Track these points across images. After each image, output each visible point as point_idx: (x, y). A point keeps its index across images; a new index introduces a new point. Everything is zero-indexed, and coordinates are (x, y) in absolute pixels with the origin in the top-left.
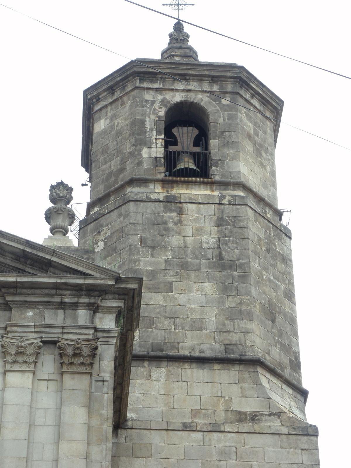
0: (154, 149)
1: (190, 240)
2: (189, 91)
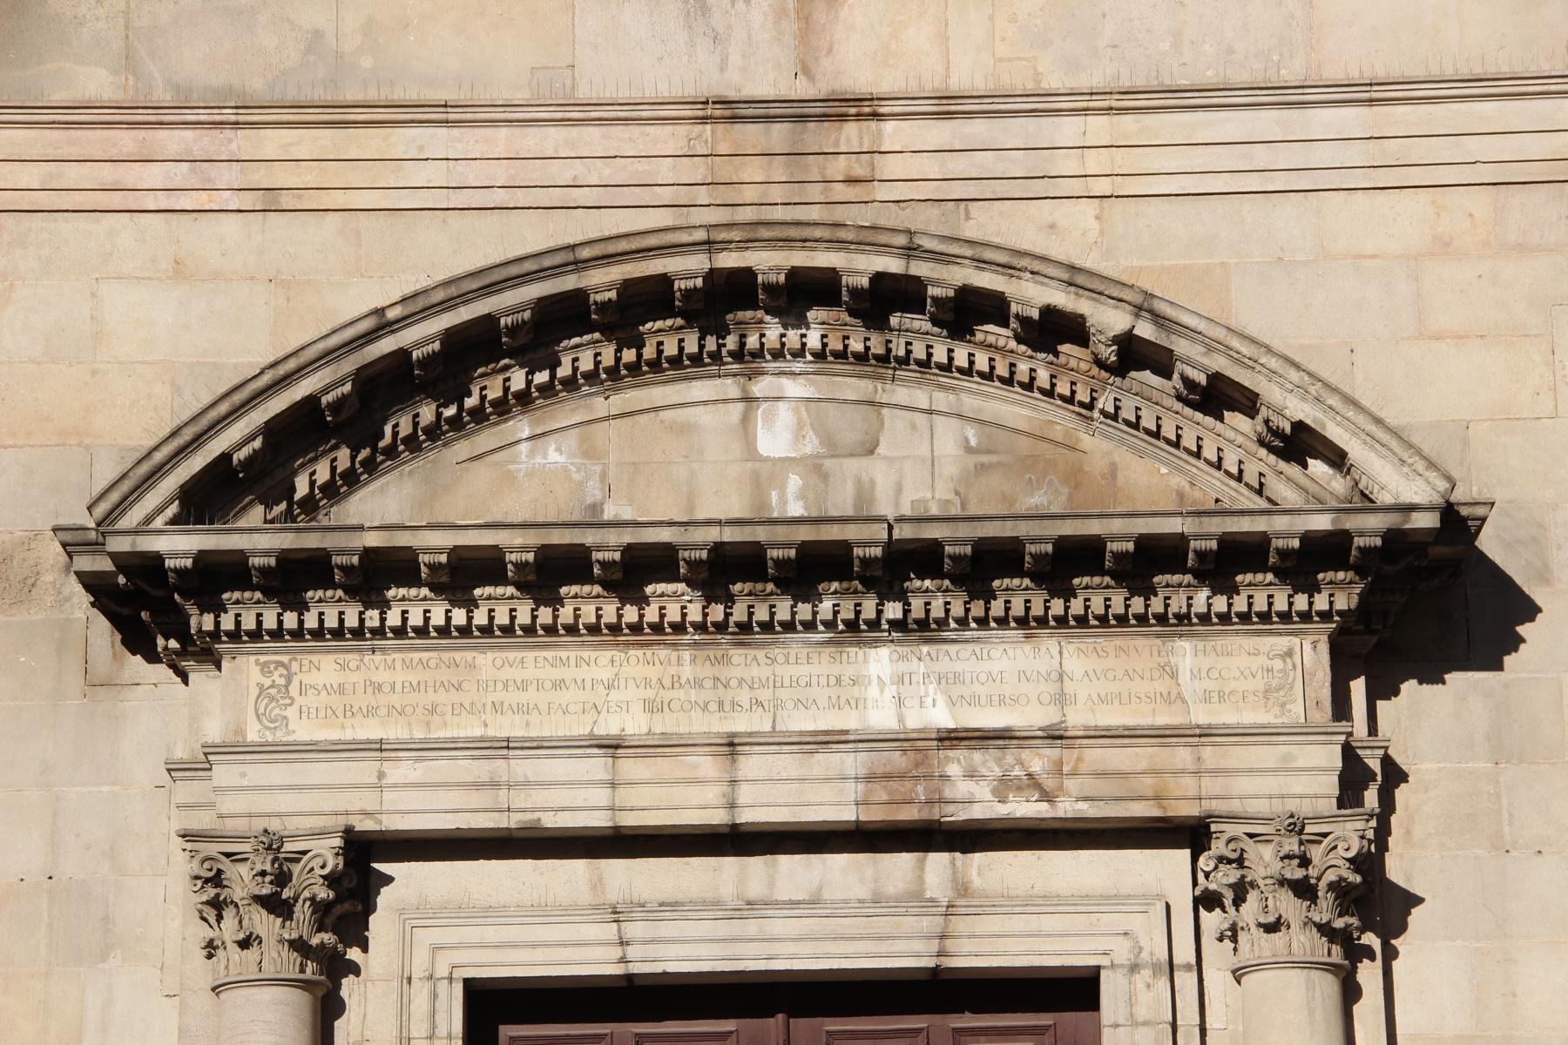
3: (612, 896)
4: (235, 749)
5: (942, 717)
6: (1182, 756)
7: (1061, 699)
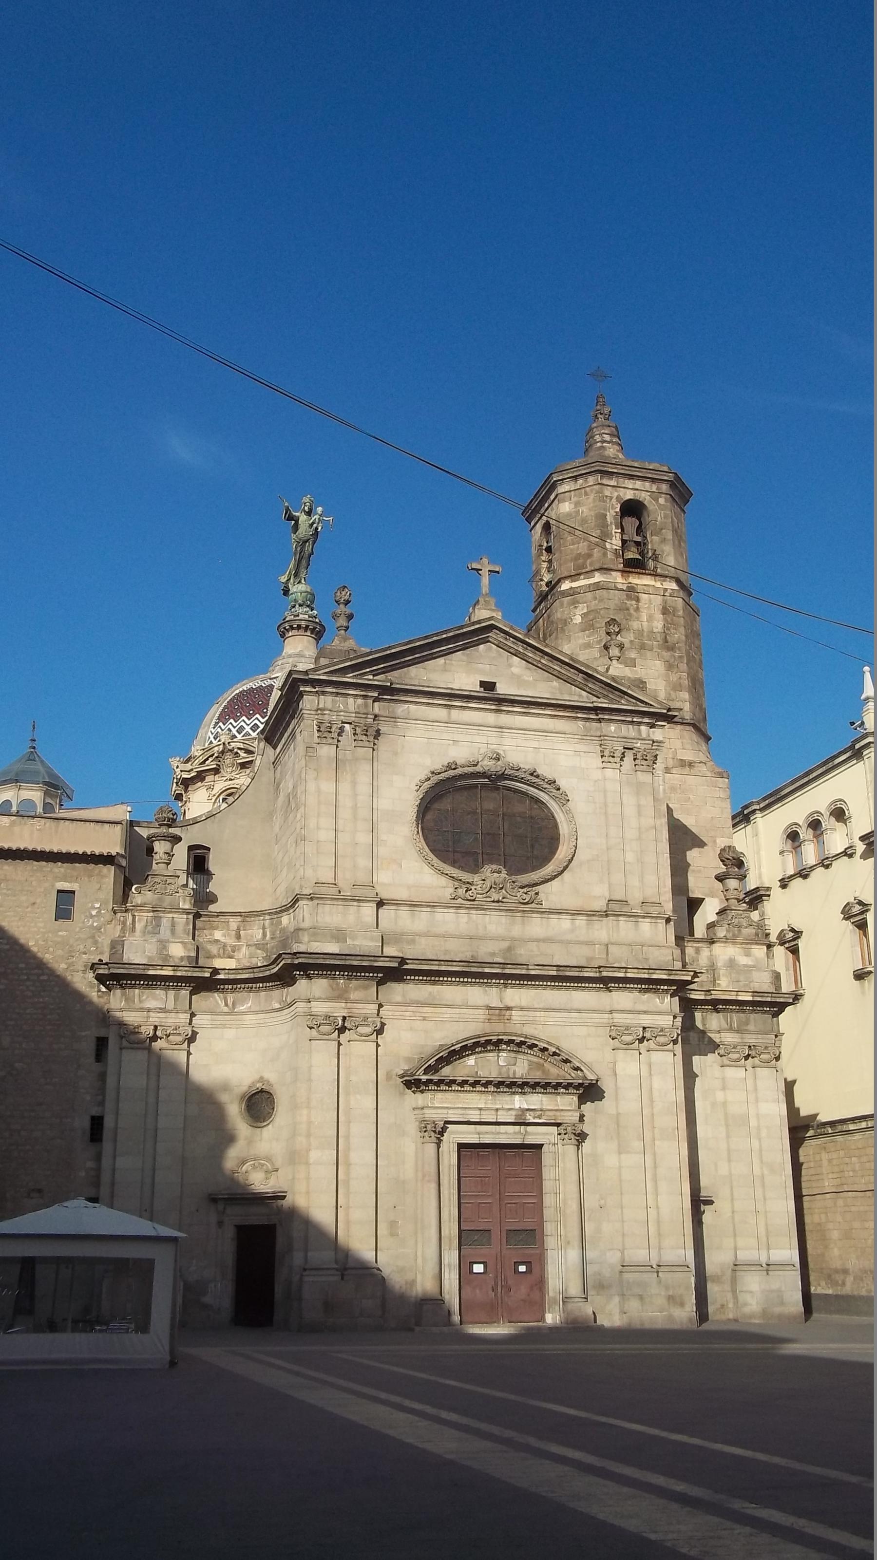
0: (614, 542)
1: (645, 624)
2: (637, 490)
3: (478, 1131)
4: (428, 1107)
5: (526, 1107)
6: (558, 1114)
7: (542, 1104)
